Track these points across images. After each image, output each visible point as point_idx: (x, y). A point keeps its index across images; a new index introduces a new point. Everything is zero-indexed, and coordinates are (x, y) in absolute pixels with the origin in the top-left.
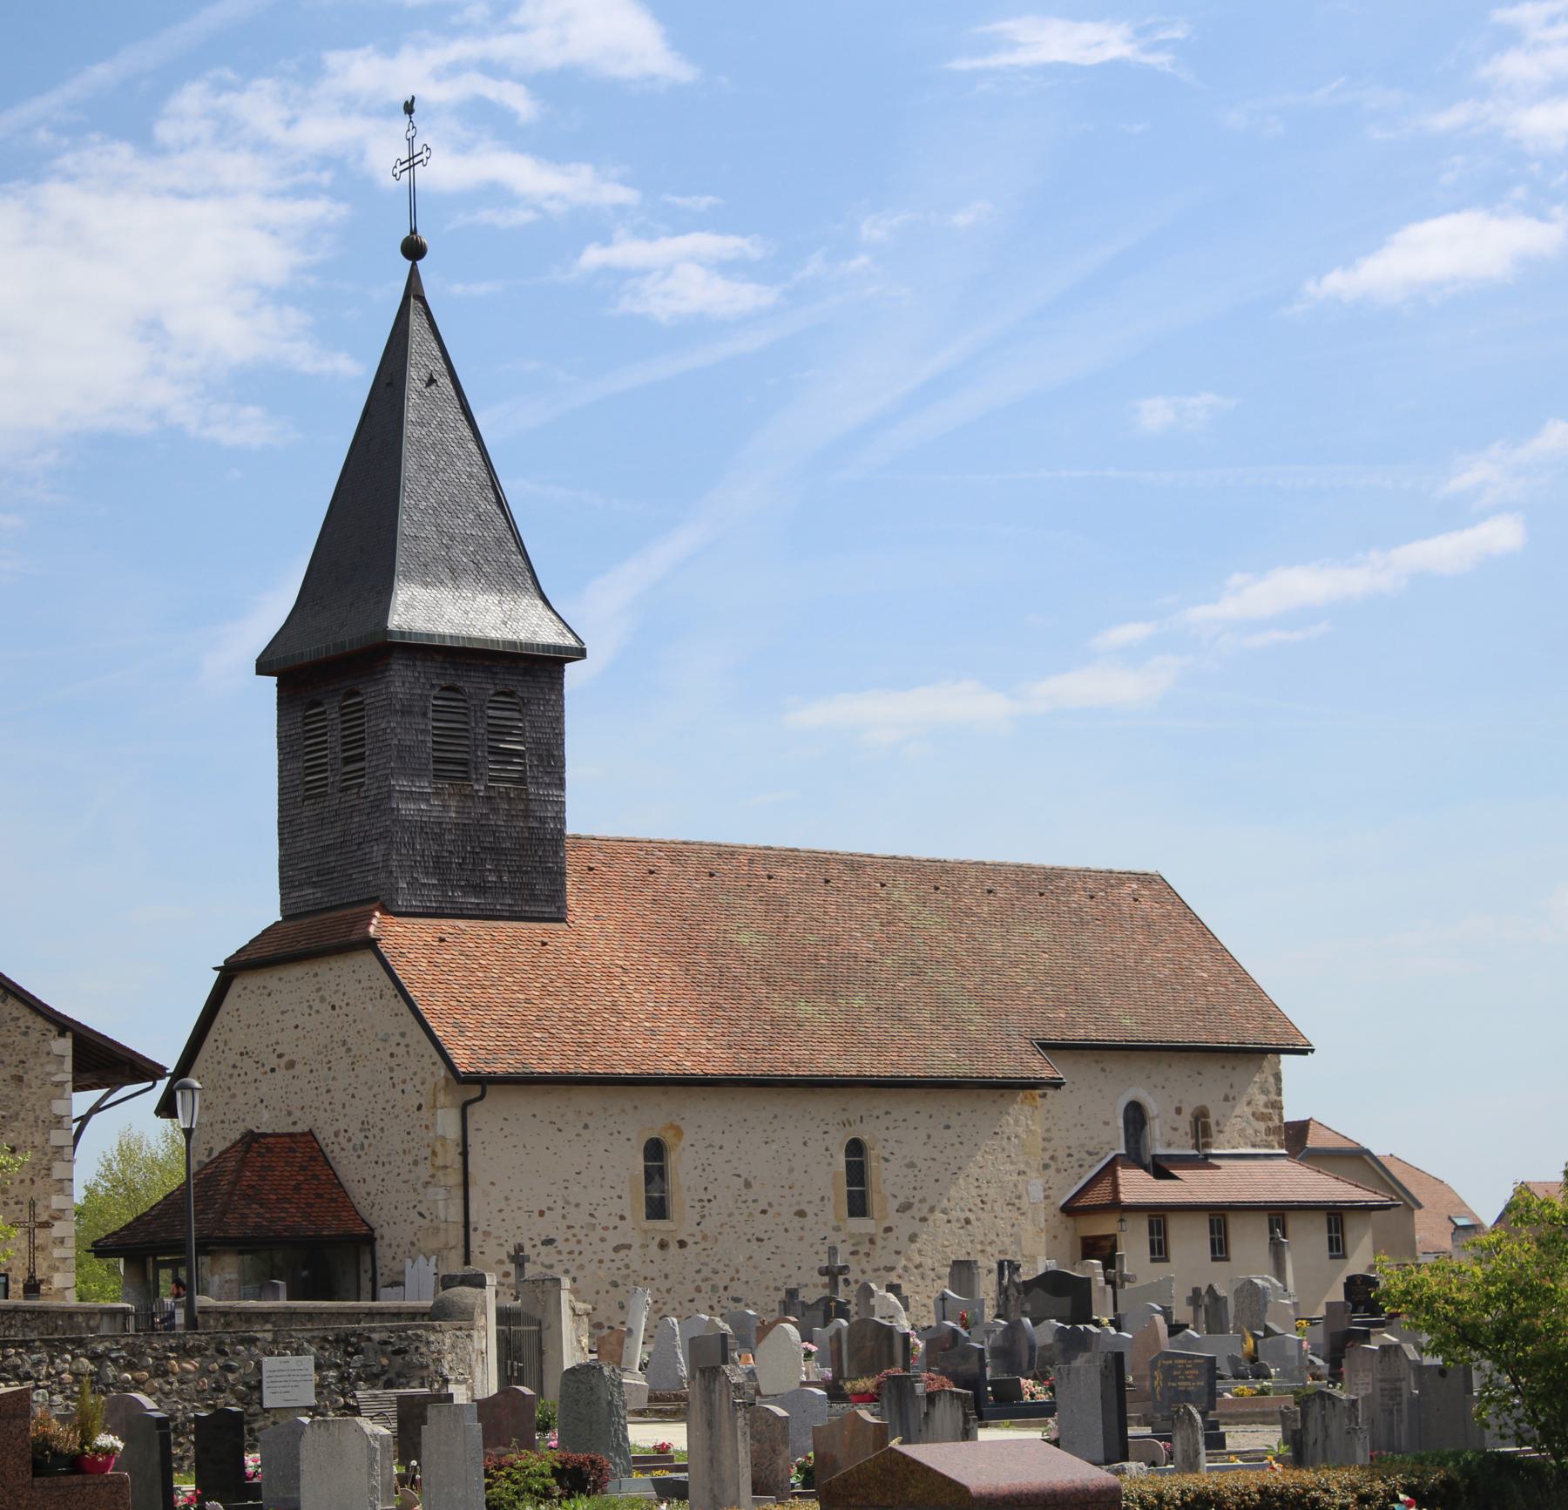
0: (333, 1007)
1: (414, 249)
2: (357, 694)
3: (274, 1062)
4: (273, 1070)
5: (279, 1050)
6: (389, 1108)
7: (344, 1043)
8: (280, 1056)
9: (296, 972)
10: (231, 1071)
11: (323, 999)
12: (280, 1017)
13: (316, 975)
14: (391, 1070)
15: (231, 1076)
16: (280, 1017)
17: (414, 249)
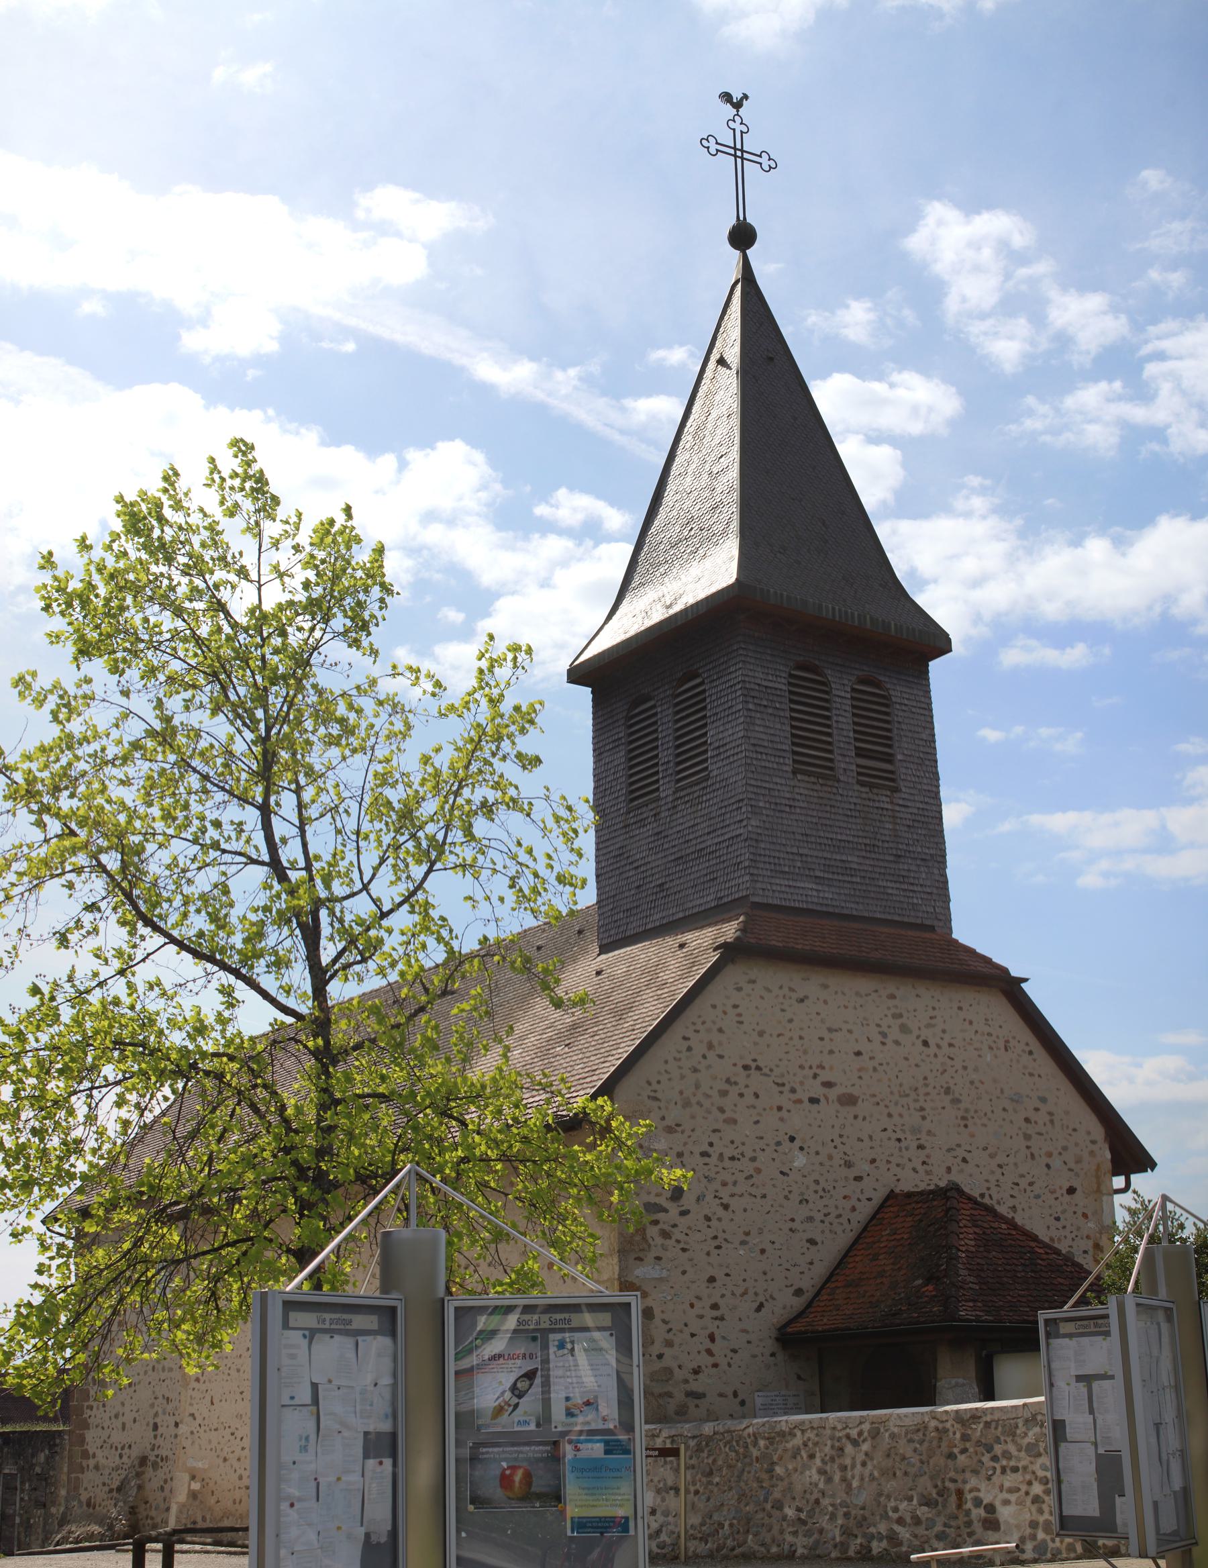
0: (925, 1043)
1: (742, 236)
2: (878, 685)
3: (818, 1091)
4: (814, 1101)
5: (825, 1076)
6: (1023, 1183)
7: (948, 1091)
8: (828, 1085)
9: (864, 984)
10: (726, 1087)
11: (904, 1029)
12: (826, 1035)
13: (892, 997)
14: (1027, 1137)
15: (723, 1093)
16: (826, 1035)
17: (742, 236)
